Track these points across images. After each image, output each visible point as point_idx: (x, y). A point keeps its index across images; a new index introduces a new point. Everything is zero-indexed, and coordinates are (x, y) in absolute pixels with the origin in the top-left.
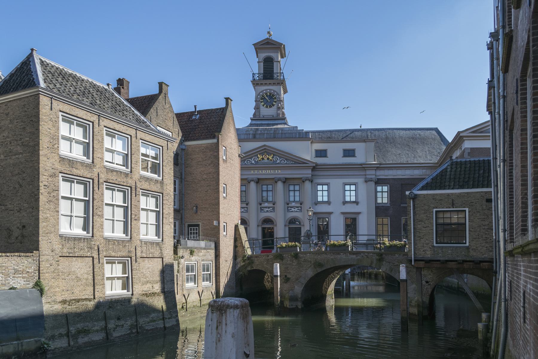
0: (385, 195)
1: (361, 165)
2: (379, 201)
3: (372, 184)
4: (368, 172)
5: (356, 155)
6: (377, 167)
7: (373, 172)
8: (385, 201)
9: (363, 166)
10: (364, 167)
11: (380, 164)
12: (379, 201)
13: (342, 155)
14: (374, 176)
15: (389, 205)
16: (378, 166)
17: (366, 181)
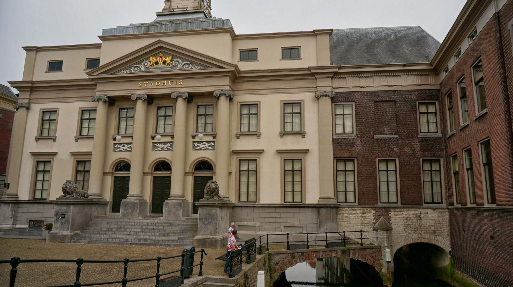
0: (348, 121)
1: (309, 69)
2: (339, 130)
3: (327, 103)
4: (321, 82)
5: (302, 55)
6: (335, 74)
7: (328, 82)
8: (349, 129)
9: (312, 71)
10: (313, 74)
11: (340, 68)
12: (339, 130)
13: (280, 57)
14: (330, 89)
15: (354, 136)
16: (336, 70)
17: (317, 98)
